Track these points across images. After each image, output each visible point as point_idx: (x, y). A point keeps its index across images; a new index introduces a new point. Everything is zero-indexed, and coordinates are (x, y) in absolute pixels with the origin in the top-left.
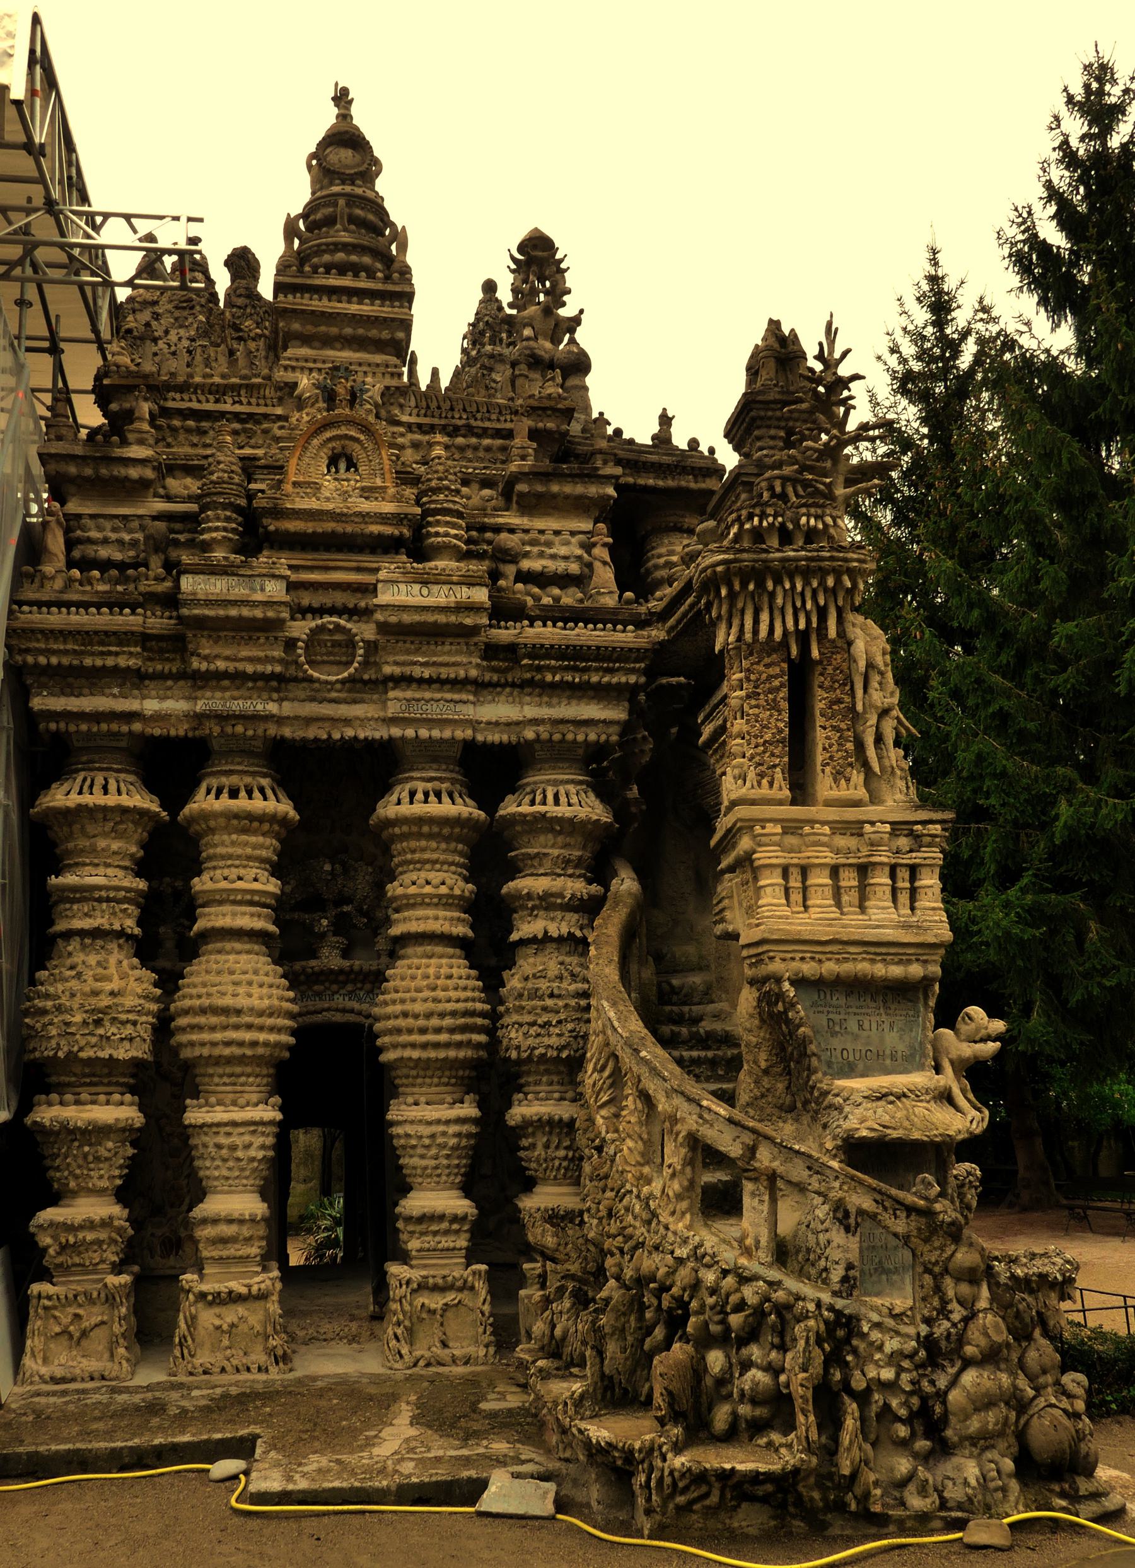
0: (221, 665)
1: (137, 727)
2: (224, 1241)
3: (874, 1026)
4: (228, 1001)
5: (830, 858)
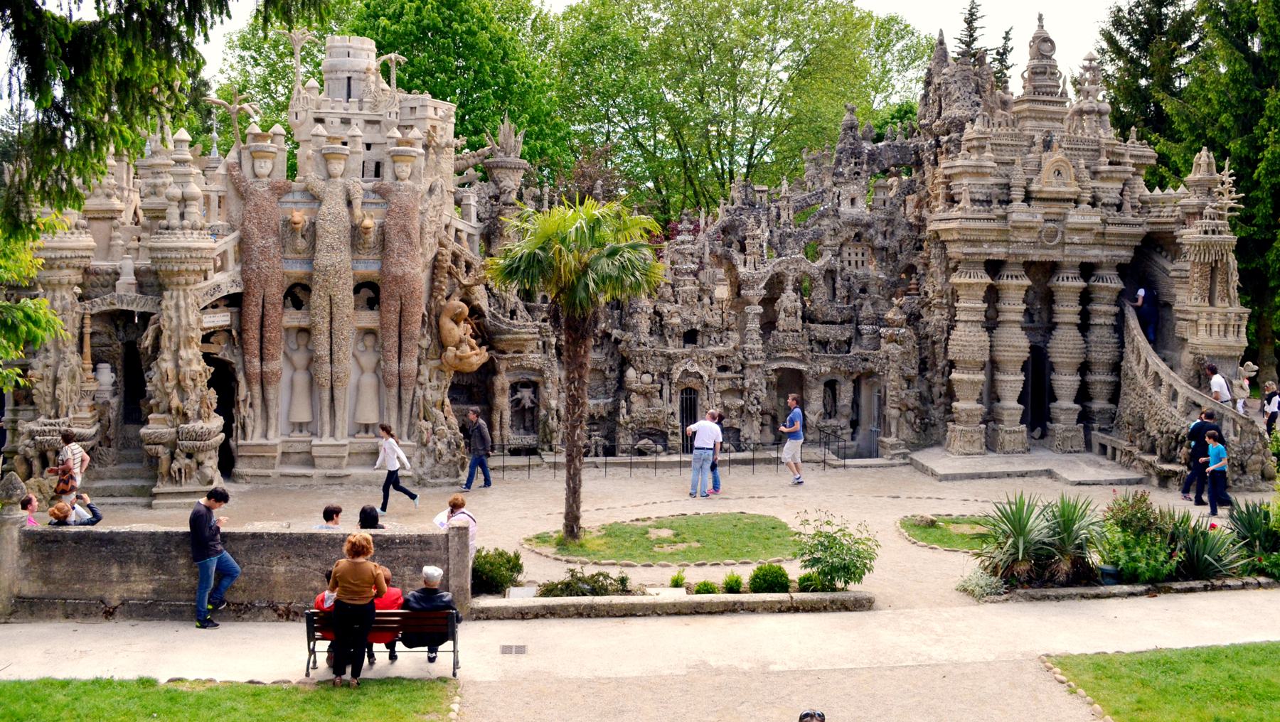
2: (1011, 415)
4: (1016, 344)
5: (1218, 322)
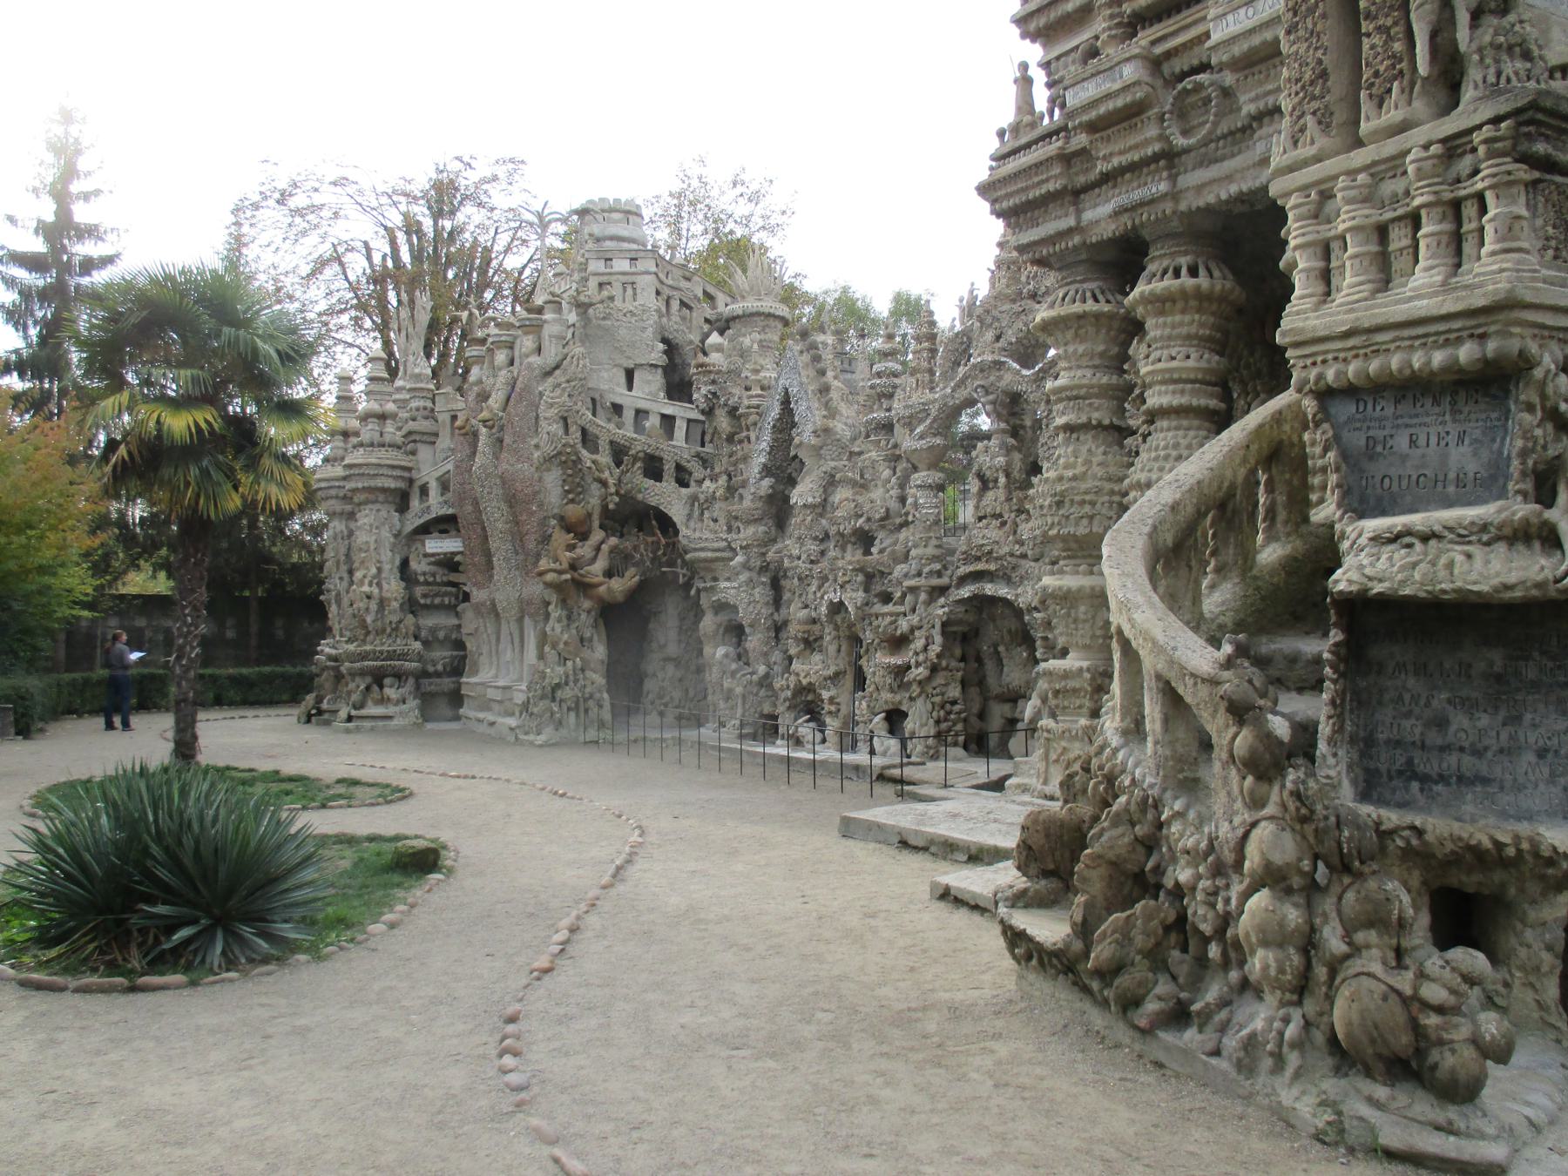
0: (1115, 161)
1: (1077, 239)
3: (1433, 440)
